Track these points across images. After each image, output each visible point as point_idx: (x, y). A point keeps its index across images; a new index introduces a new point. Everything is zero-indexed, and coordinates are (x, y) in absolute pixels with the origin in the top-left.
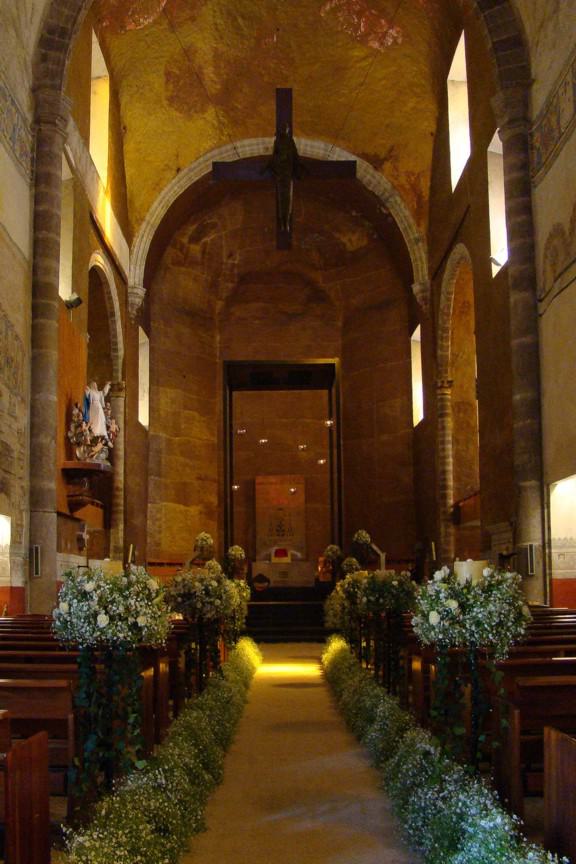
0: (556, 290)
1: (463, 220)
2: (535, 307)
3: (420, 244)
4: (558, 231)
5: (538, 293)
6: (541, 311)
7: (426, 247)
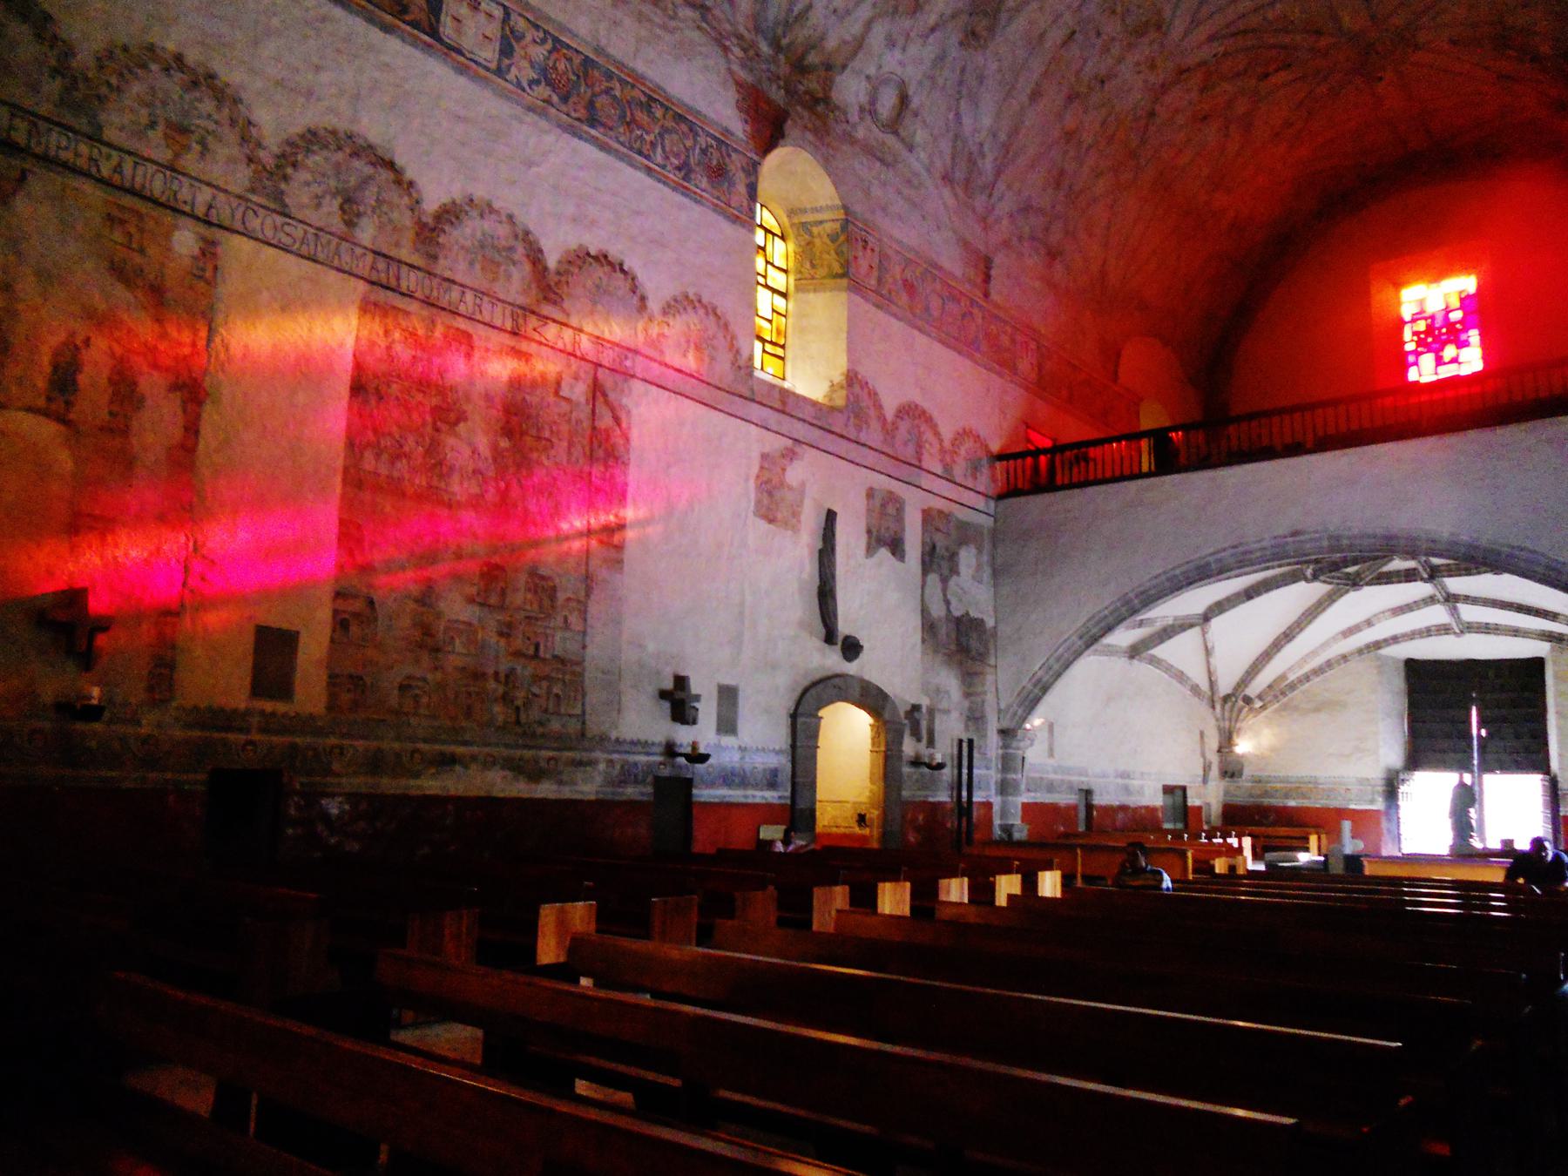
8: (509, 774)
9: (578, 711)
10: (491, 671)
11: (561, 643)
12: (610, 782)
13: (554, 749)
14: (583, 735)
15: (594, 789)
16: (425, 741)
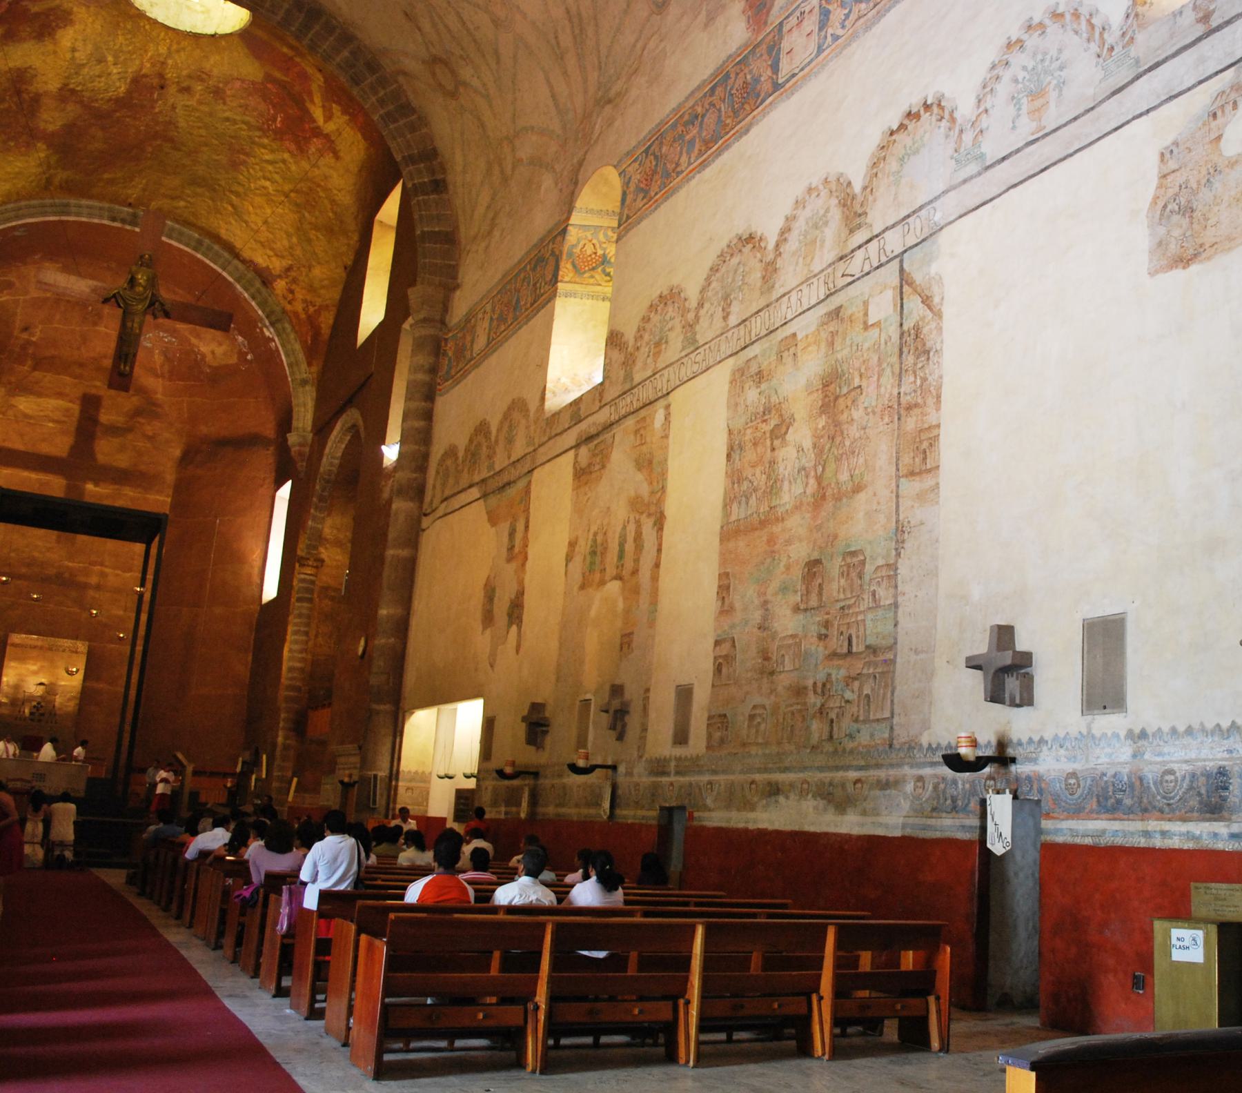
0: (441, 514)
1: (363, 385)
2: (419, 522)
3: (308, 388)
4: (451, 452)
5: (425, 506)
6: (424, 525)
7: (314, 394)
8: (821, 803)
9: (887, 714)
10: (810, 683)
11: (873, 628)
12: (919, 812)
13: (860, 768)
14: (891, 746)
15: (901, 820)
16: (759, 771)
